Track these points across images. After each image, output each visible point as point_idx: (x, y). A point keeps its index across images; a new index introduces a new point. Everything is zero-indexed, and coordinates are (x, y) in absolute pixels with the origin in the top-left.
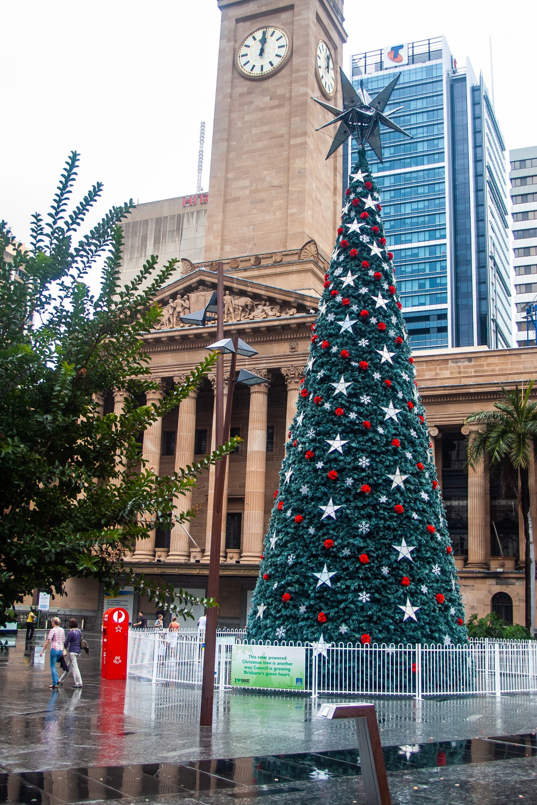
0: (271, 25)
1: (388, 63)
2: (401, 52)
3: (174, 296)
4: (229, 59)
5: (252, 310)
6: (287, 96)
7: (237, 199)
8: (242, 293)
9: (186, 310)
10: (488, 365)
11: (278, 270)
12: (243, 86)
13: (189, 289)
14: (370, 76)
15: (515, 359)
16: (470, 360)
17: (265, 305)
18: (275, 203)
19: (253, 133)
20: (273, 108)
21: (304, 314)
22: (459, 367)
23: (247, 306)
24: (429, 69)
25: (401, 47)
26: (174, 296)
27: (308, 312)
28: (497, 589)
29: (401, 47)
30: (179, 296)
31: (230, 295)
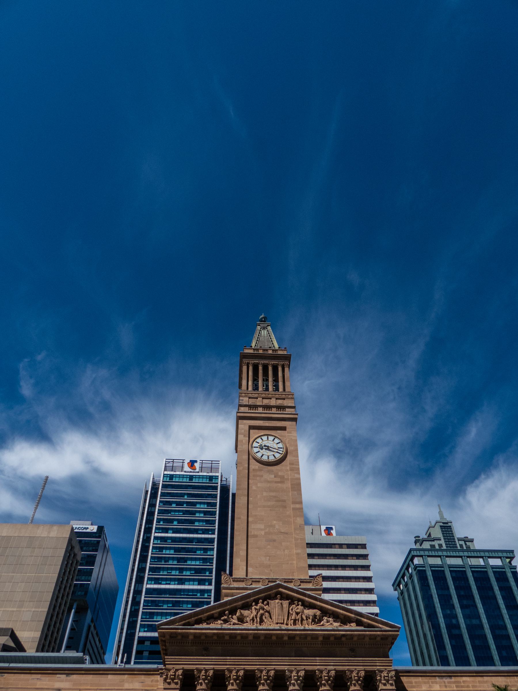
0: (273, 434)
1: (187, 468)
2: (195, 464)
5: (320, 620)
6: (286, 477)
7: (255, 536)
8: (311, 606)
10: (464, 682)
14: (175, 473)
15: (480, 679)
17: (329, 617)
19: (264, 495)
20: (277, 482)
22: (445, 682)
23: (315, 616)
24: (211, 478)
25: (196, 461)
29: (196, 461)
30: (261, 601)
31: (302, 606)
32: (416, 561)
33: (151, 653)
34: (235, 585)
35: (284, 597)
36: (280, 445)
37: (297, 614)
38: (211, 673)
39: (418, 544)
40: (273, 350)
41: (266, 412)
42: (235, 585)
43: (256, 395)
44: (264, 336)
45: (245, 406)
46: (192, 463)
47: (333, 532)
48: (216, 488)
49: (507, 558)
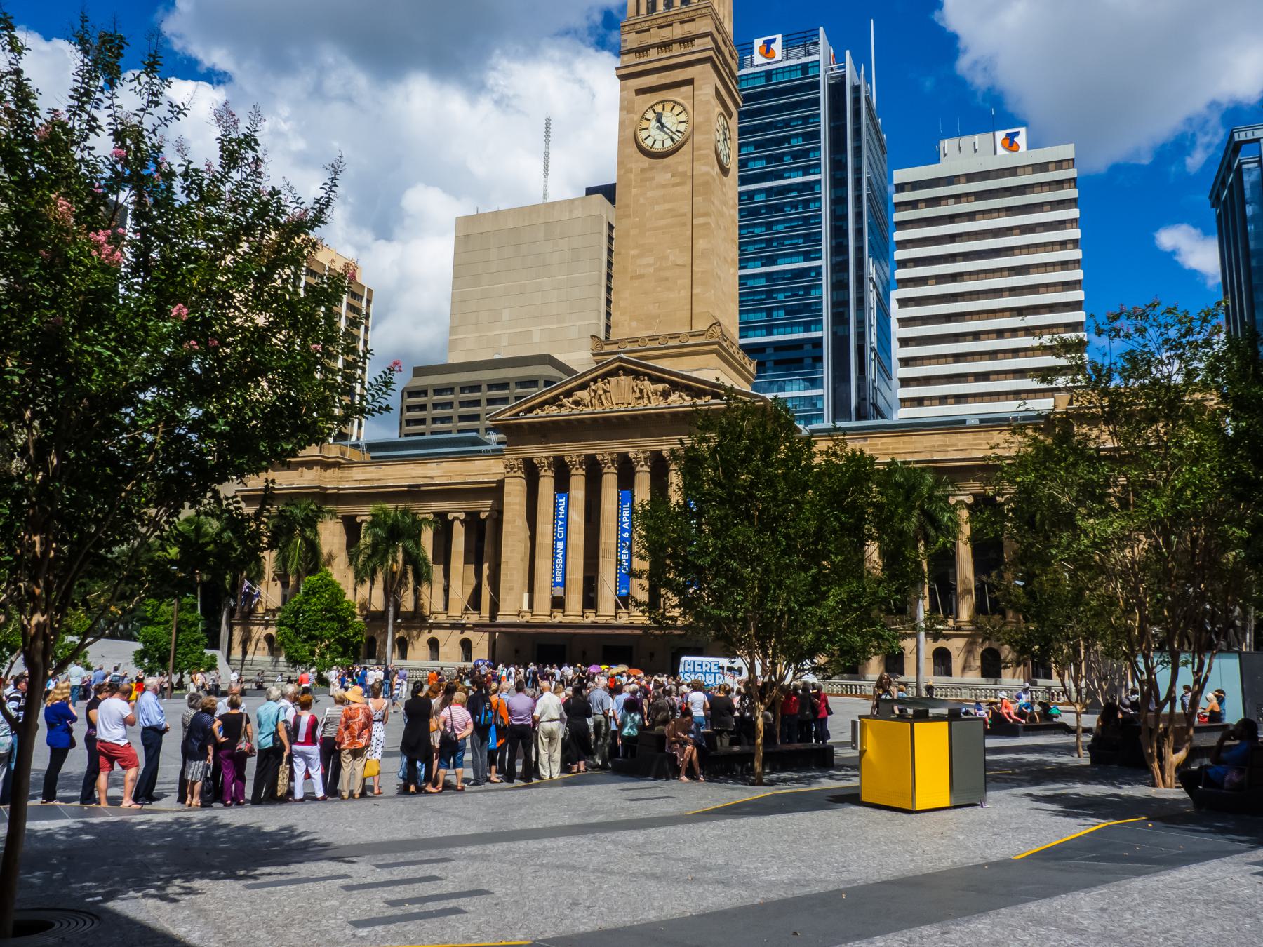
3: (595, 380)
4: (629, 132)
7: (641, 276)
12: (647, 162)
18: (679, 282)
21: (718, 401)
24: (805, 68)
25: (774, 40)
26: (595, 380)
35: (628, 372)
37: (641, 391)
41: (664, 55)
42: (607, 349)
43: (647, 24)
45: (630, 51)
46: (767, 49)
47: (1021, 140)
48: (816, 86)
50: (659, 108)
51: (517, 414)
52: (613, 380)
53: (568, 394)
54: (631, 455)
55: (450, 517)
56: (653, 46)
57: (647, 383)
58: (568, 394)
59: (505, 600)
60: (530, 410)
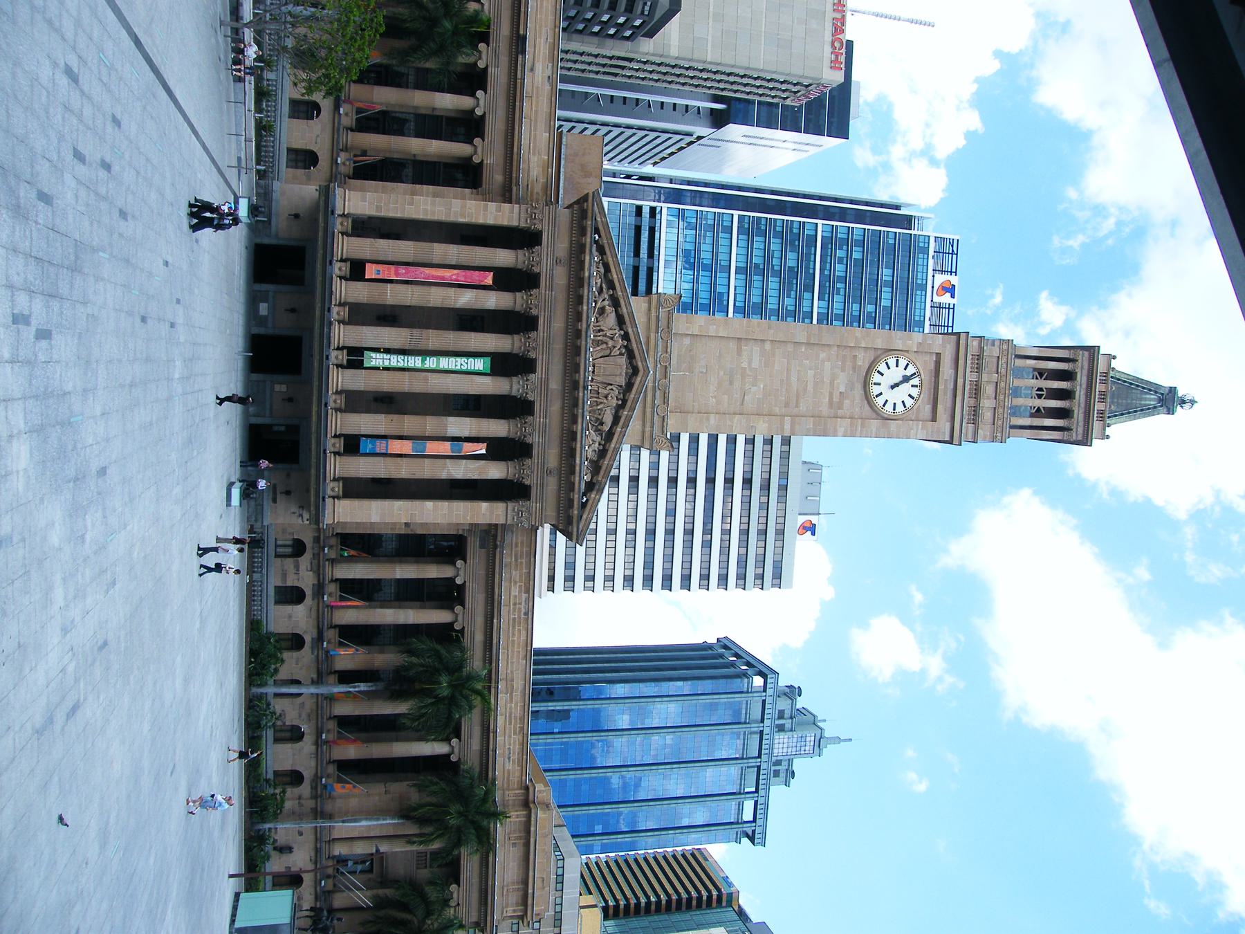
1: (940, 279)
2: (948, 295)
3: (626, 337)
6: (840, 412)
9: (607, 352)
11: (649, 410)
12: (863, 360)
13: (631, 355)
15: (522, 654)
16: (526, 614)
23: (602, 424)
25: (953, 296)
26: (626, 337)
27: (584, 494)
28: (308, 639)
29: (953, 296)
32: (758, 681)
33: (638, 229)
34: (663, 315)
36: (900, 408)
38: (536, 270)
39: (787, 690)
40: (1101, 412)
42: (663, 315)
44: (1141, 399)
46: (951, 290)
49: (754, 831)
50: (916, 381)
51: (597, 231)
52: (623, 360)
53: (615, 303)
54: (532, 376)
55: (480, 93)
56: (980, 377)
57: (614, 402)
58: (615, 303)
59: (364, 200)
60: (601, 251)
